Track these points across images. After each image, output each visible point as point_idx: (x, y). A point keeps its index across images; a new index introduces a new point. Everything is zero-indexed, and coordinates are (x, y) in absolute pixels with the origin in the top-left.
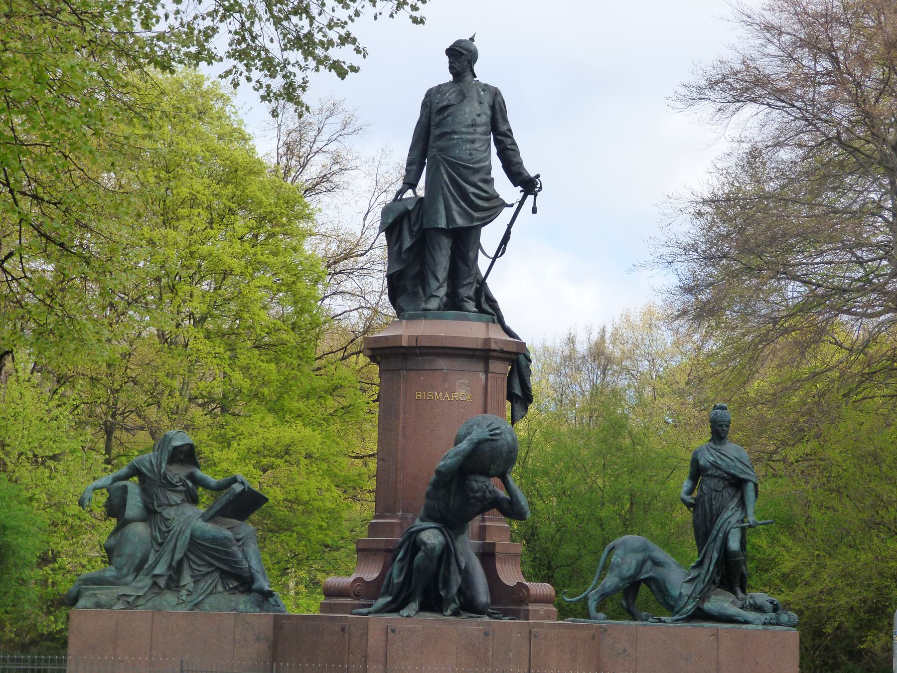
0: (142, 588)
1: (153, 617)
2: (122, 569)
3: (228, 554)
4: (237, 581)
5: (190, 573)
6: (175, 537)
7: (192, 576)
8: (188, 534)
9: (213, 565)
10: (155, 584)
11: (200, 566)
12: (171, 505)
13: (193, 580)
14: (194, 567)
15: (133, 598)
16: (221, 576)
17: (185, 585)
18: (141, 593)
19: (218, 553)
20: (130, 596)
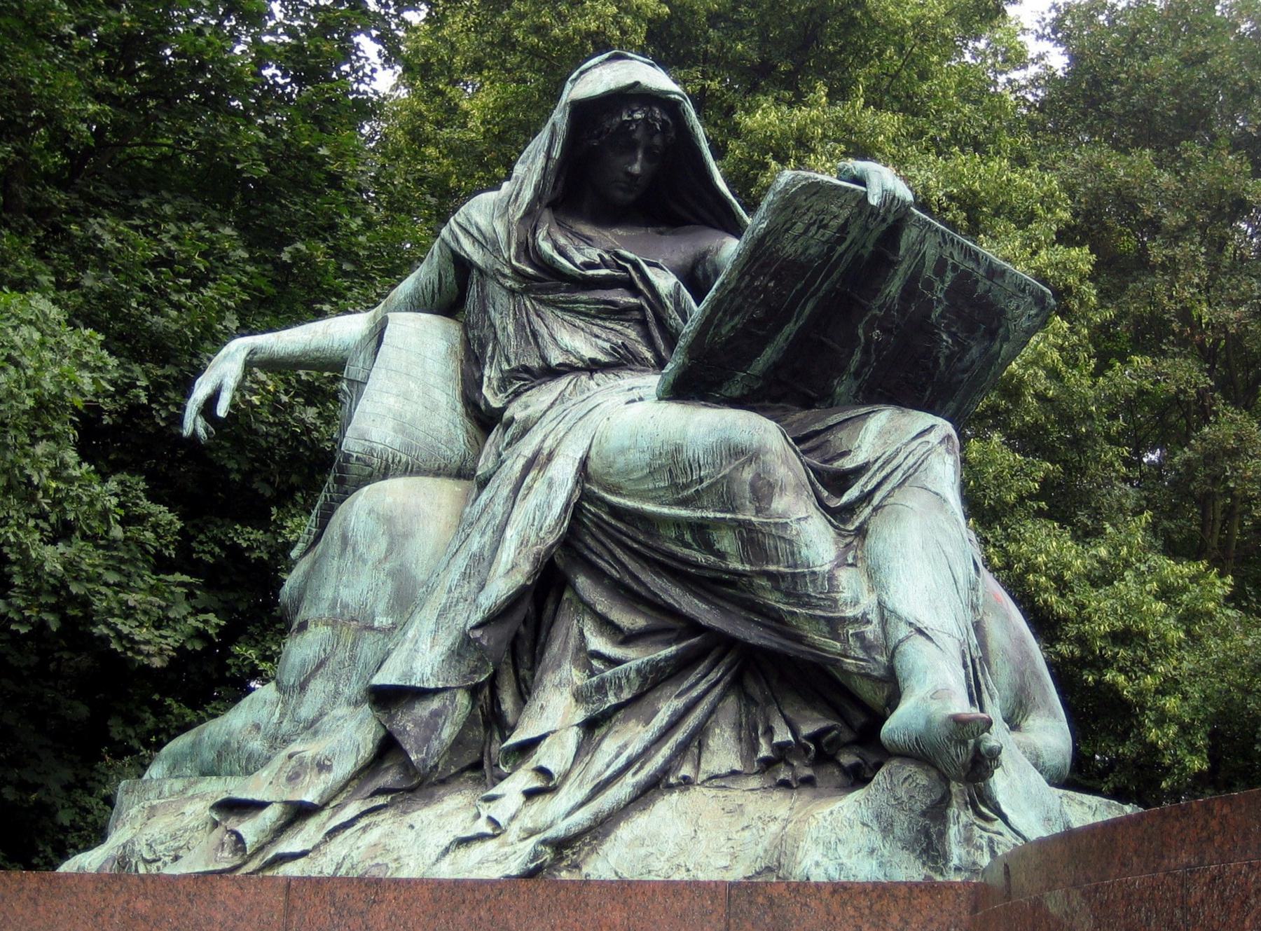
0: (322, 766)
1: (289, 909)
2: (303, 687)
3: (751, 539)
4: (838, 712)
5: (578, 677)
6: (505, 491)
7: (580, 696)
8: (563, 471)
9: (694, 626)
10: (388, 747)
11: (628, 638)
12: (551, 373)
13: (580, 715)
14: (597, 643)
15: (270, 816)
16: (736, 684)
17: (528, 747)
18: (310, 796)
19: (708, 547)
20: (261, 806)
